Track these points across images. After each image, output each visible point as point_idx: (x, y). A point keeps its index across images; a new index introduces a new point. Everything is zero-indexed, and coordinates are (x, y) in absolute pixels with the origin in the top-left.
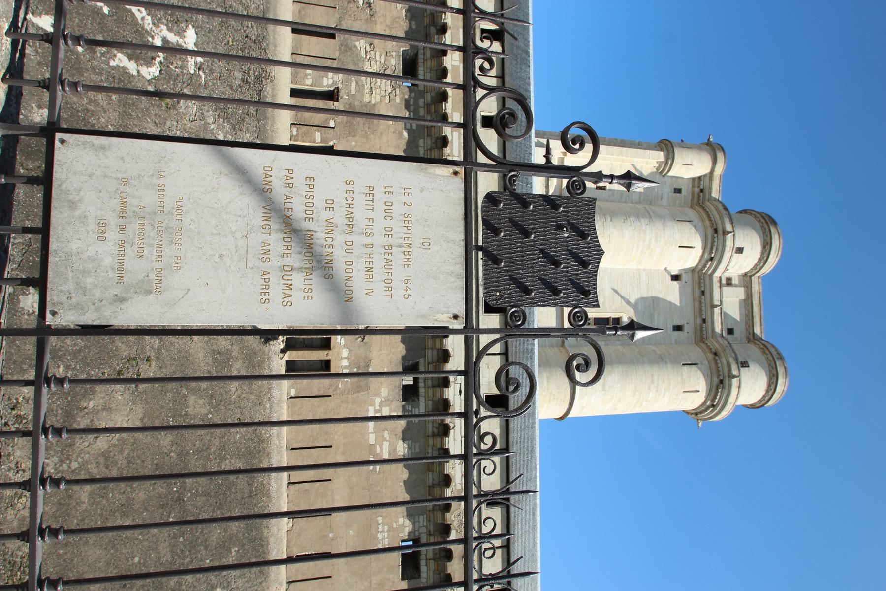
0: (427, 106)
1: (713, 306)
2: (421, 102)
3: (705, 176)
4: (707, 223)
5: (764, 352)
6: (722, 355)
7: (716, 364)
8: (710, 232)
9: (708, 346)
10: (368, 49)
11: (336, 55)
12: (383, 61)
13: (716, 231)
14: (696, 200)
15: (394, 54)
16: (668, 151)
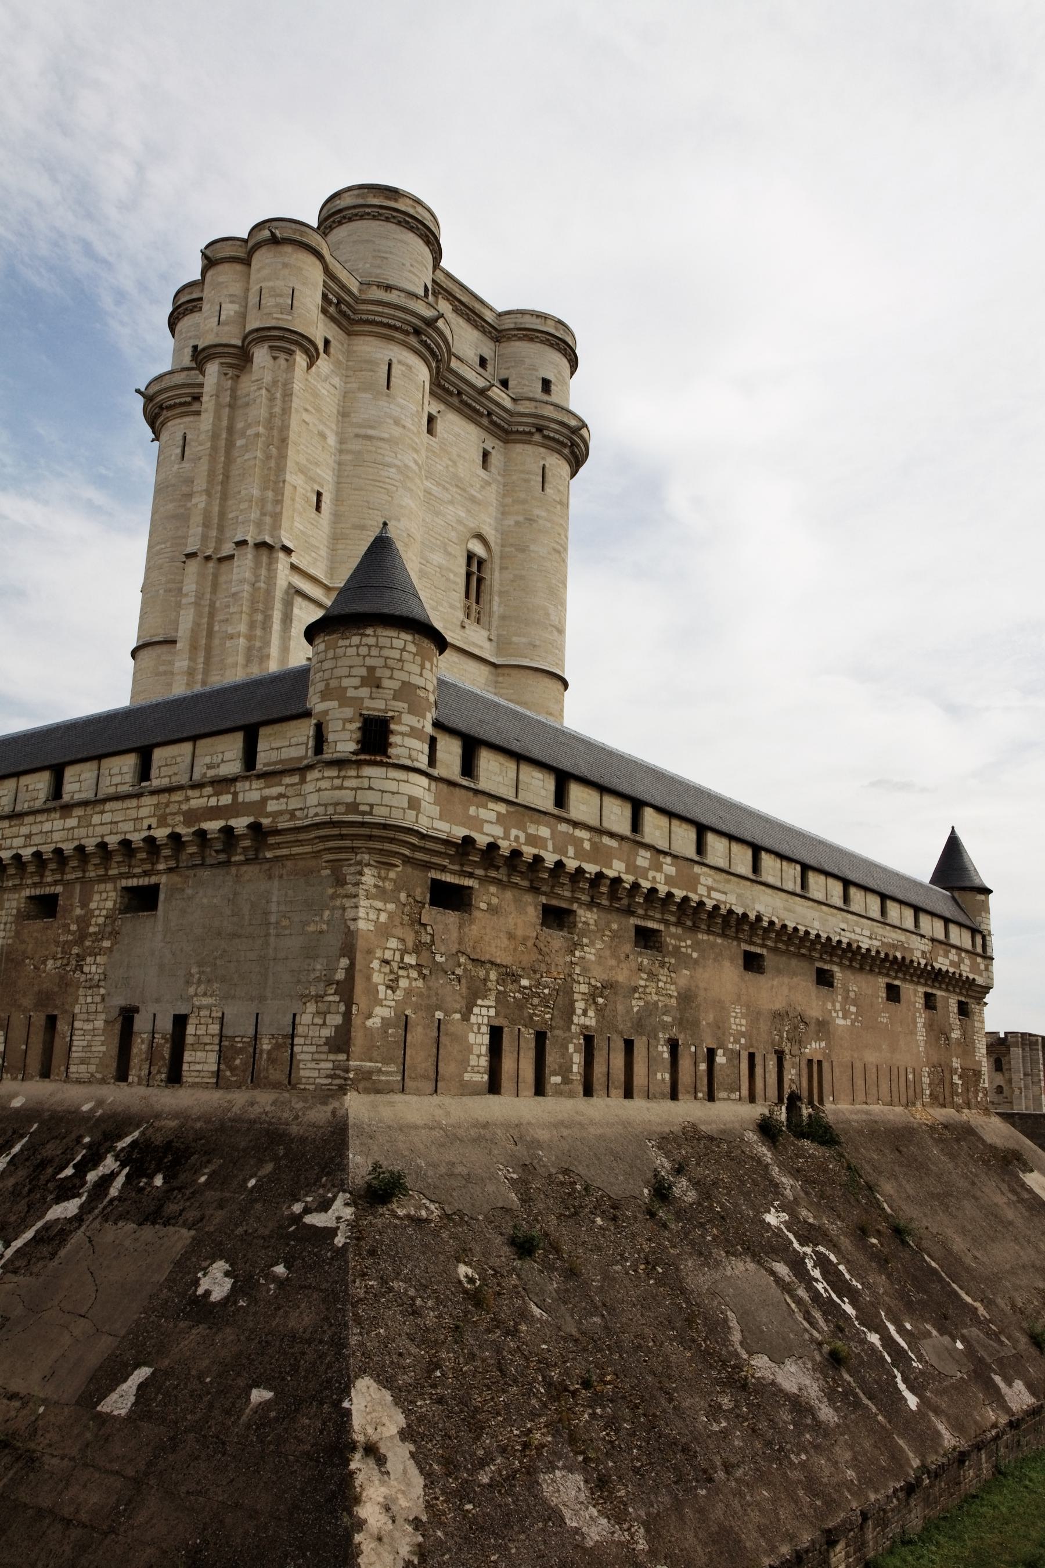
0: (679, 923)
1: (482, 392)
2: (673, 929)
3: (325, 284)
4: (397, 335)
5: (531, 340)
6: (546, 423)
7: (553, 439)
8: (413, 340)
9: (524, 433)
10: (637, 995)
11: (644, 1038)
12: (645, 976)
13: (417, 332)
14: (345, 323)
15: (640, 960)
16: (296, 343)
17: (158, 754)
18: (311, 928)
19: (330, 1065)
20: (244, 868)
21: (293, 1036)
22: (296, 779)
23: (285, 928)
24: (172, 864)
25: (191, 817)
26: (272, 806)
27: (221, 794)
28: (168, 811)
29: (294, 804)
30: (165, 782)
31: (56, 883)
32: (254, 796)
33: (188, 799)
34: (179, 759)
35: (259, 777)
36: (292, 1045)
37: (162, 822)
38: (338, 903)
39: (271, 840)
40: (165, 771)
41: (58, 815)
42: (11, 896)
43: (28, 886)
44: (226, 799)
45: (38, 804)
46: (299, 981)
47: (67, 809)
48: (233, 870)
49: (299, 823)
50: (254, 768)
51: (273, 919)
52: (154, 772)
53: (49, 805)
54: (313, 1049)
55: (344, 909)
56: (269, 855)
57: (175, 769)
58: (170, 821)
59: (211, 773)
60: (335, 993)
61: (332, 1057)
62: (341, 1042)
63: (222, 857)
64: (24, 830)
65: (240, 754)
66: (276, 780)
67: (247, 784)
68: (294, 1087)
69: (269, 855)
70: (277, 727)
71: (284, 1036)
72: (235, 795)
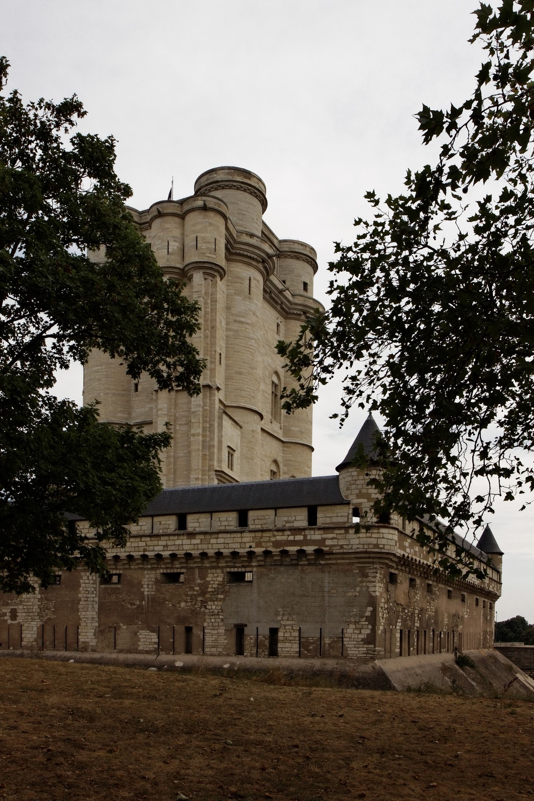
17: (252, 515)
18: (350, 594)
19: (365, 649)
20: (306, 567)
21: (342, 638)
22: (343, 531)
23: (334, 593)
24: (262, 563)
25: (276, 544)
26: (328, 542)
27: (296, 535)
28: (262, 540)
29: (341, 543)
30: (259, 527)
31: (182, 568)
32: (318, 537)
33: (274, 536)
34: (266, 517)
35: (319, 529)
36: (343, 641)
37: (259, 545)
38: (364, 584)
39: (327, 557)
40: (257, 522)
41: (185, 537)
42: (149, 572)
43: (161, 568)
44: (300, 538)
45: (169, 531)
46: (344, 615)
47: (192, 535)
48: (300, 568)
49: (345, 551)
50: (316, 524)
51: (326, 589)
52: (250, 522)
53: (177, 532)
54: (355, 643)
55: (368, 587)
56: (322, 562)
57: (265, 521)
58: (263, 544)
59: (288, 525)
60: (365, 621)
61: (365, 646)
62: (371, 639)
63: (294, 562)
64: (164, 543)
65: (307, 518)
66: (331, 531)
67: (312, 532)
68: (345, 658)
69: (322, 562)
70: (328, 507)
71: (339, 638)
72: (305, 536)
